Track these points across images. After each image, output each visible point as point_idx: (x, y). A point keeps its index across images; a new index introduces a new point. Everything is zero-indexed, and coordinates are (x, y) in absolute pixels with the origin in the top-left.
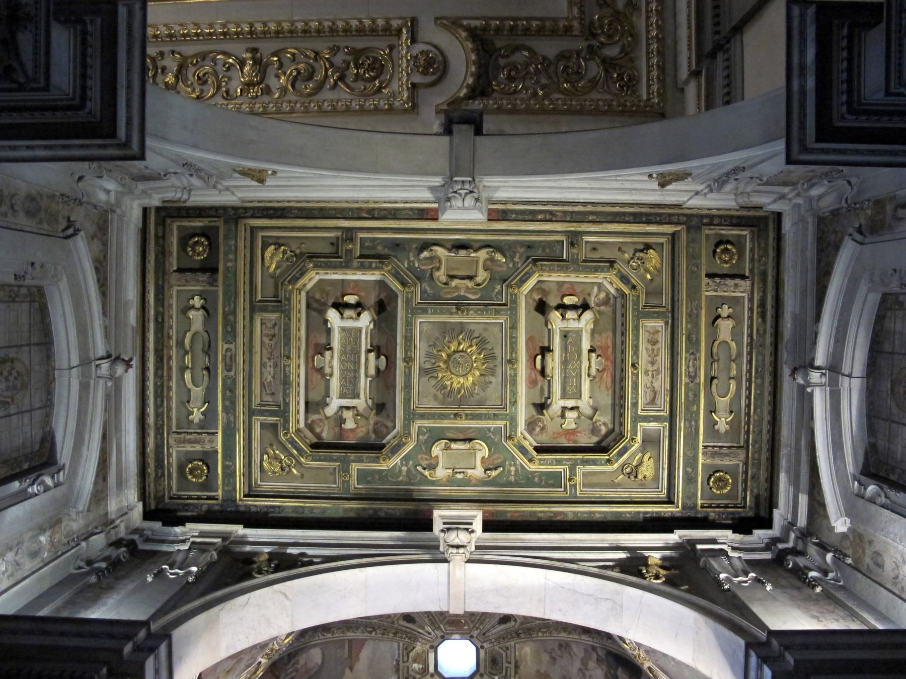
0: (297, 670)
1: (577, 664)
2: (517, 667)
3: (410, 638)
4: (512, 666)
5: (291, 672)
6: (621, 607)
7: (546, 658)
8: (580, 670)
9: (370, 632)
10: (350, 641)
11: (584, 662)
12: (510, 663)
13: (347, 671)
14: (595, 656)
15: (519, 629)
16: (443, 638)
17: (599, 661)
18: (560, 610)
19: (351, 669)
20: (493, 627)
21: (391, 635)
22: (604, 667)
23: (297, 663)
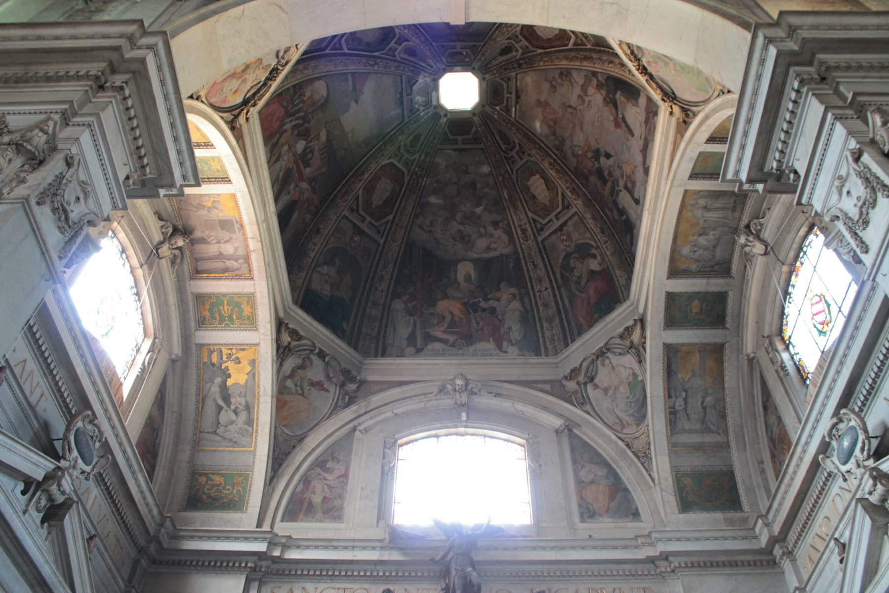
0: (303, 102)
1: (577, 91)
2: (518, 97)
3: (412, 72)
4: (513, 96)
5: (298, 104)
6: (627, 10)
7: (546, 86)
8: (579, 96)
9: (373, 66)
10: (353, 74)
11: (584, 88)
12: (511, 93)
13: (353, 103)
14: (595, 82)
15: (520, 59)
16: (445, 71)
17: (599, 86)
18: (564, 17)
19: (356, 102)
20: (495, 58)
21: (393, 69)
22: (603, 92)
23: (302, 95)
